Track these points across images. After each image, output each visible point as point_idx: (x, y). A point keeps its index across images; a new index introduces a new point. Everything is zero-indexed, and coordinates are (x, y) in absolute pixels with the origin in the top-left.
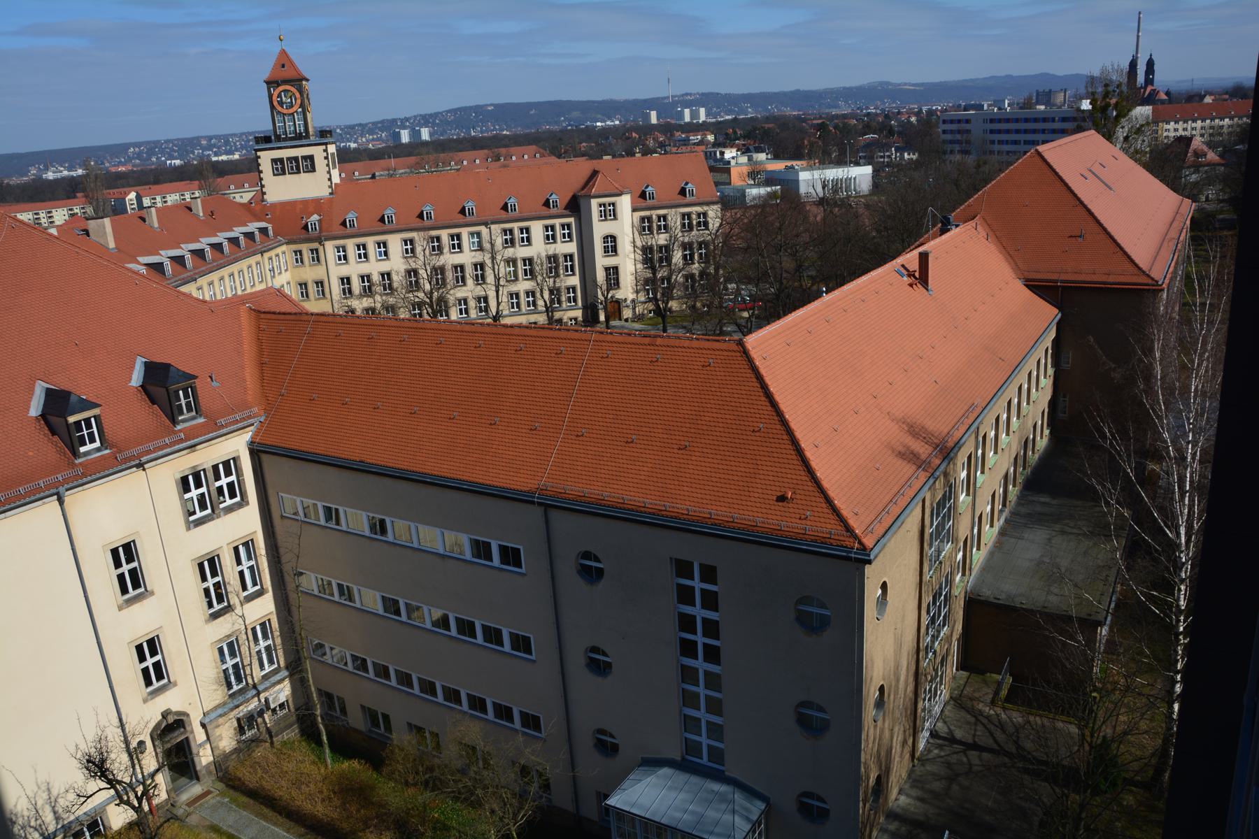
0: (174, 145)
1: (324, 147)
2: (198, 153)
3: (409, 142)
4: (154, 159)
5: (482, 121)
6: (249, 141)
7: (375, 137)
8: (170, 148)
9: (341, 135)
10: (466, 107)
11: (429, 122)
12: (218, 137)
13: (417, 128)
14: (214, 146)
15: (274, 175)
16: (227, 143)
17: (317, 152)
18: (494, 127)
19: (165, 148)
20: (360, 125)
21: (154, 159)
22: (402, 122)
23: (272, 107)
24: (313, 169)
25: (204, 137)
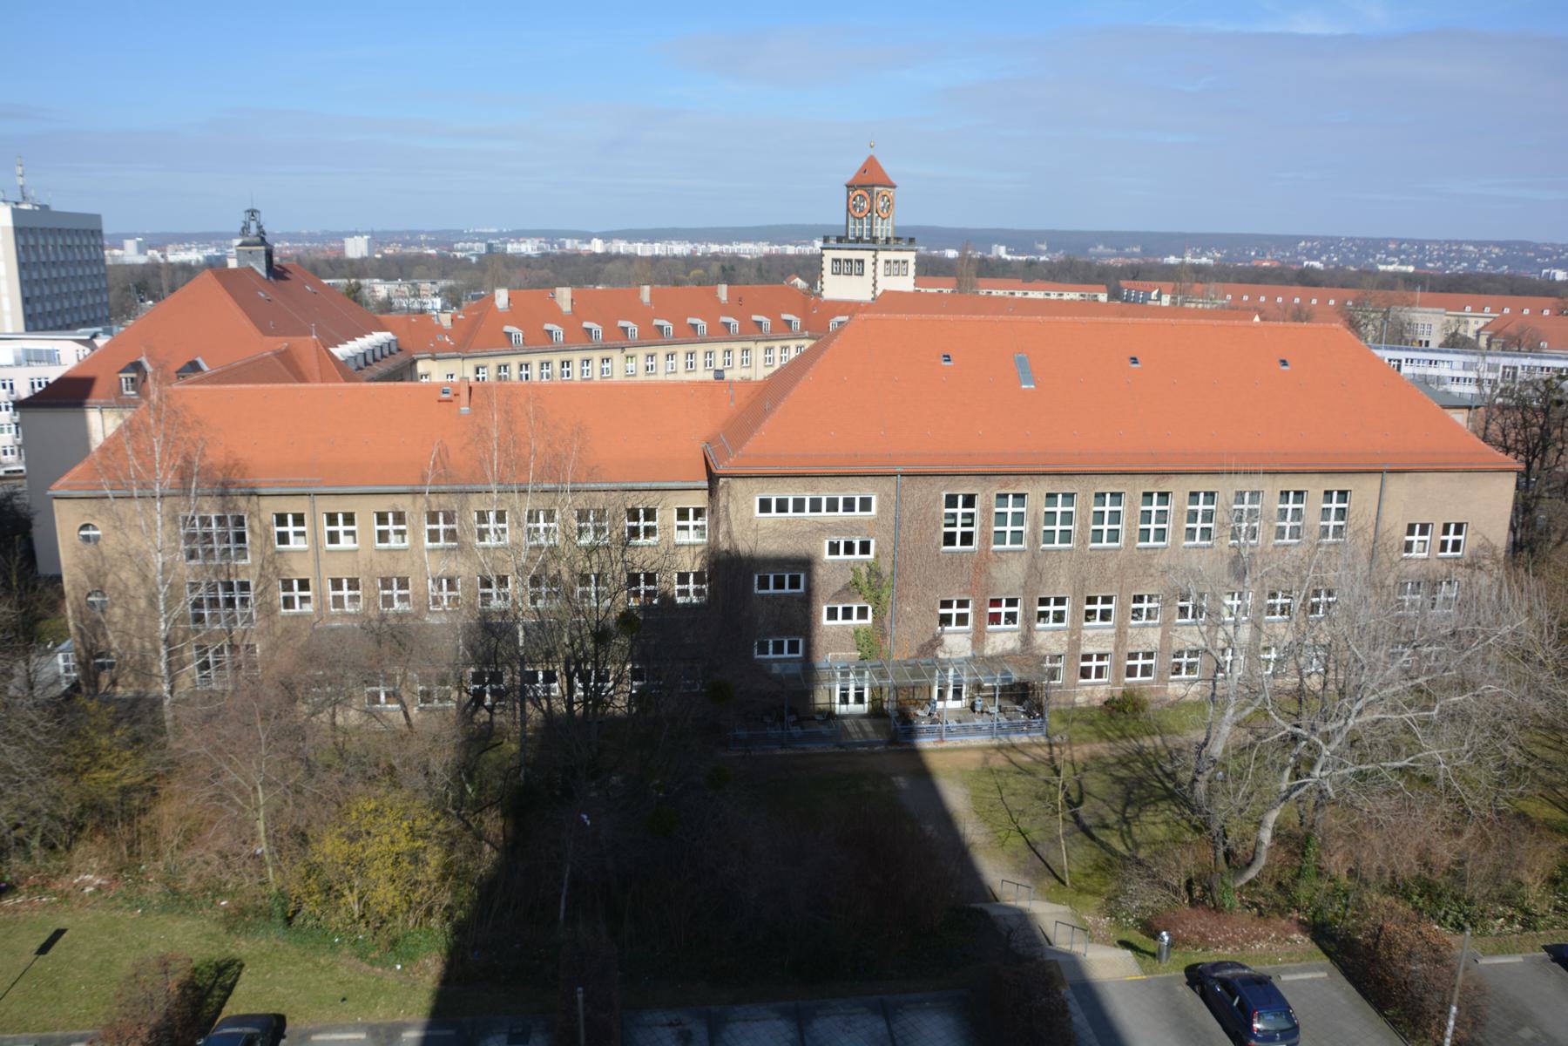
0: (1354, 245)
6: (1450, 251)
12: (1411, 242)
14: (1404, 252)
16: (1421, 250)
19: (1343, 247)
25: (1394, 240)
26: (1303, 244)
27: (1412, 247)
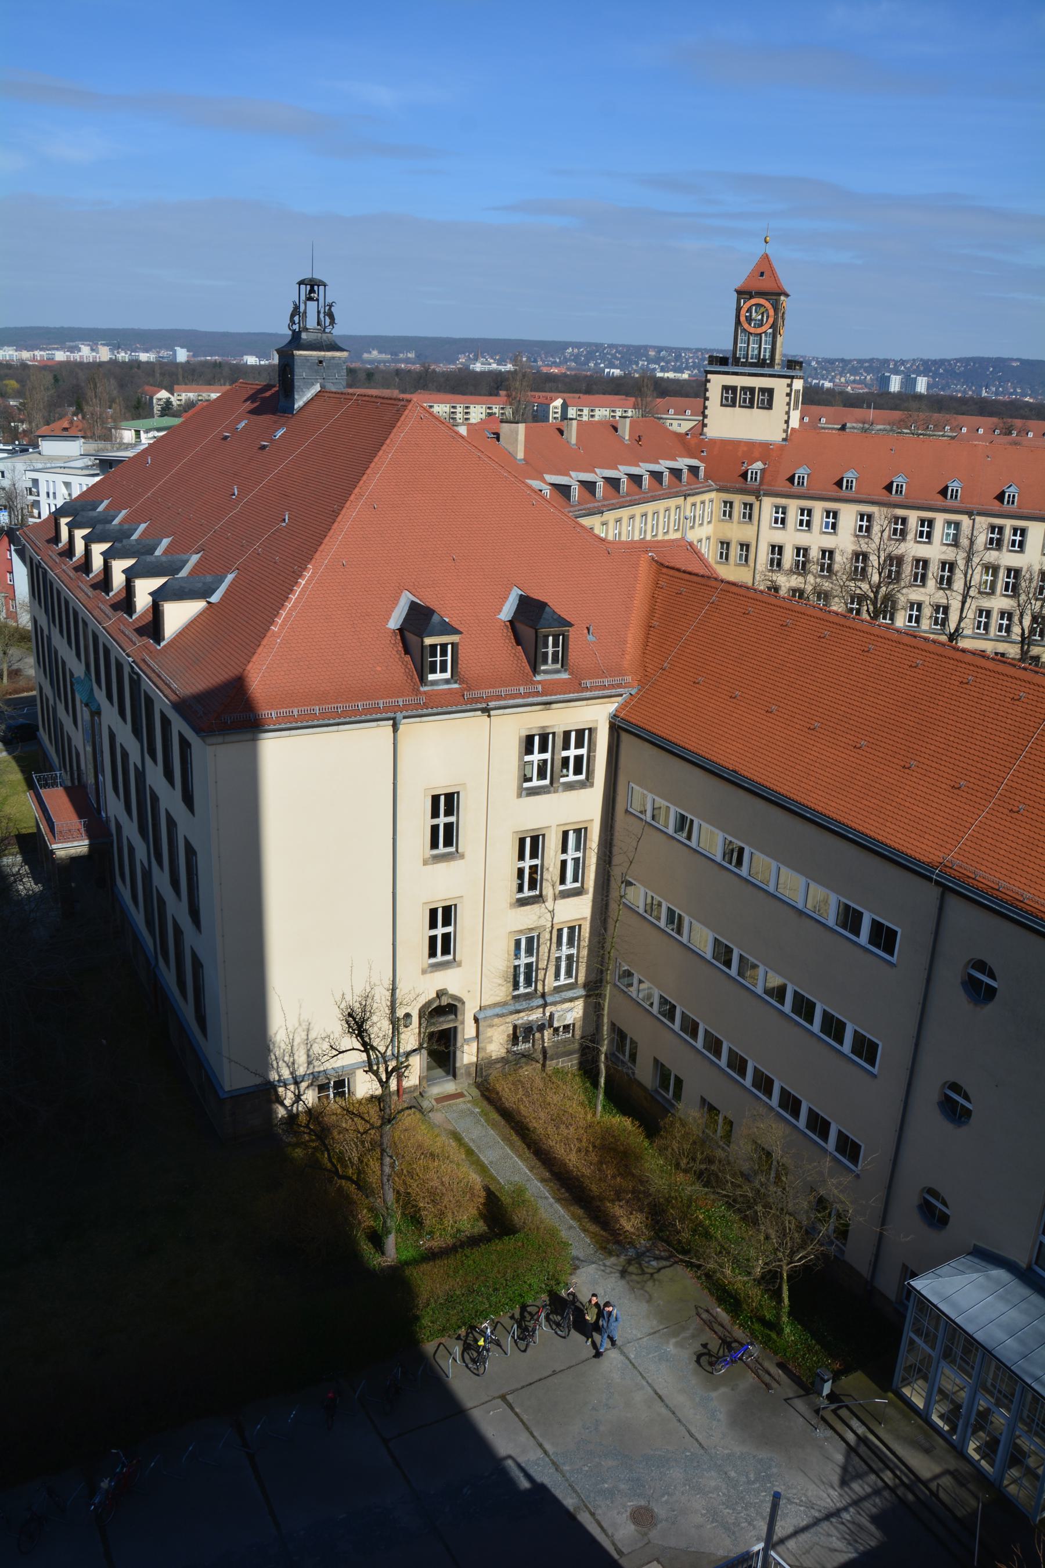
1: (789, 381)
2: (643, 365)
3: (899, 392)
4: (592, 365)
5: (1000, 379)
6: (703, 359)
7: (858, 378)
8: (612, 355)
9: (815, 369)
10: (983, 358)
11: (930, 371)
12: (669, 350)
13: (913, 376)
14: (663, 359)
15: (722, 405)
16: (678, 357)
17: (779, 386)
18: (1015, 391)
19: (607, 353)
20: (842, 360)
21: (592, 365)
22: (895, 365)
23: (738, 322)
24: (770, 407)
25: (654, 347)
26: (570, 350)
27: (670, 355)
